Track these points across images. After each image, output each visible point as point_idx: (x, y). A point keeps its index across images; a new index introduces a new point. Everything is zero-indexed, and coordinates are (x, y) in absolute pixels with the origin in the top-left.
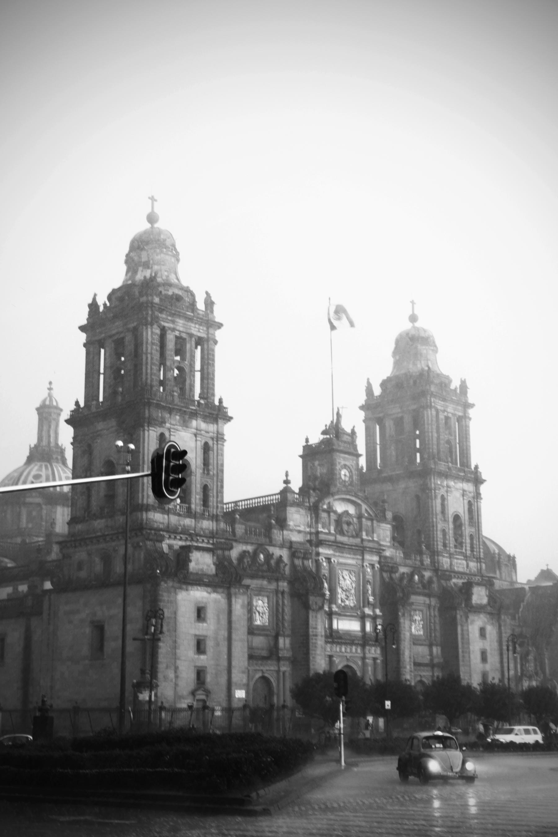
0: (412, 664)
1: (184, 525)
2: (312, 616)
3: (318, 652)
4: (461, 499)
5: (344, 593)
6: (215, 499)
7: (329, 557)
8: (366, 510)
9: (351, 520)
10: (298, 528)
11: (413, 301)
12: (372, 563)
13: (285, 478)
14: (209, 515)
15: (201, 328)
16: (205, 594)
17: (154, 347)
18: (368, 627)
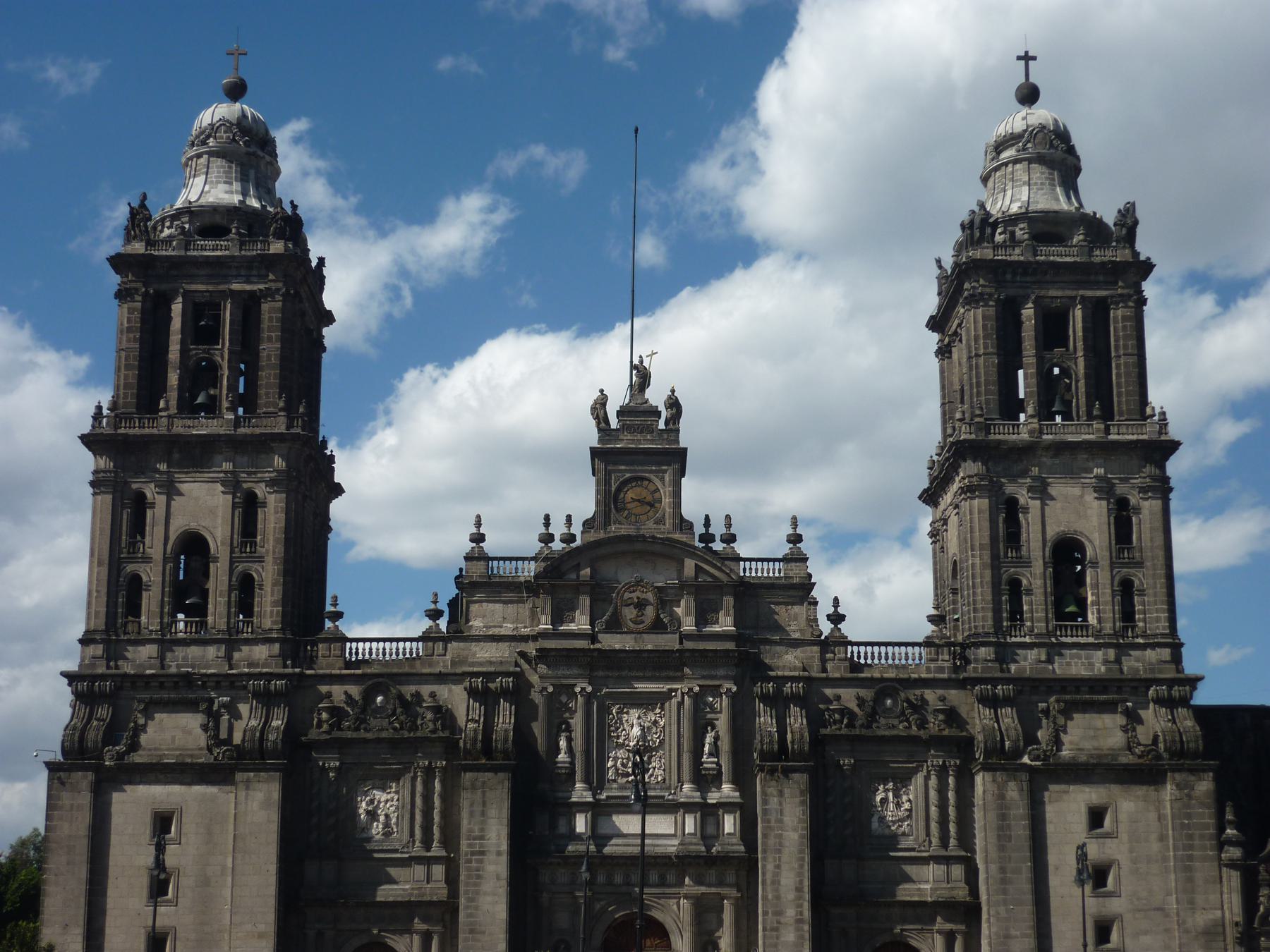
0: (806, 905)
1: (185, 658)
2: (471, 814)
3: (488, 886)
4: (1090, 497)
6: (269, 599)
7: (572, 682)
9: (650, 596)
10: (496, 631)
11: (1027, 52)
13: (474, 530)
14: (252, 633)
15: (254, 272)
16: (176, 788)
17: (131, 335)
18: (690, 824)
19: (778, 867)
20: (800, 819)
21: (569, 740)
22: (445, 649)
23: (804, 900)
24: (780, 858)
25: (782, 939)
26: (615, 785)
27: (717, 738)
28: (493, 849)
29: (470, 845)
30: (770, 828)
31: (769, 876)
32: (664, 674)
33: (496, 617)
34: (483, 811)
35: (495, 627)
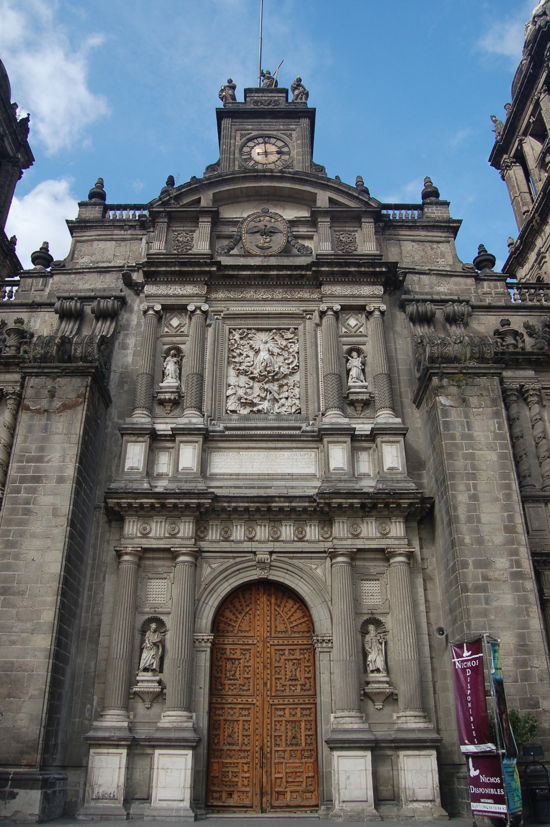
2: (30, 429)
5: (257, 385)
7: (183, 301)
8: (331, 200)
12: (361, 302)
19: (474, 497)
20: (496, 434)
21: (179, 364)
22: (45, 285)
23: (519, 544)
24: (475, 486)
25: (495, 604)
26: (235, 416)
27: (364, 364)
28: (54, 475)
29: (21, 469)
30: (455, 445)
31: (462, 513)
32: (297, 295)
33: (107, 254)
34: (46, 425)
35: (103, 262)
